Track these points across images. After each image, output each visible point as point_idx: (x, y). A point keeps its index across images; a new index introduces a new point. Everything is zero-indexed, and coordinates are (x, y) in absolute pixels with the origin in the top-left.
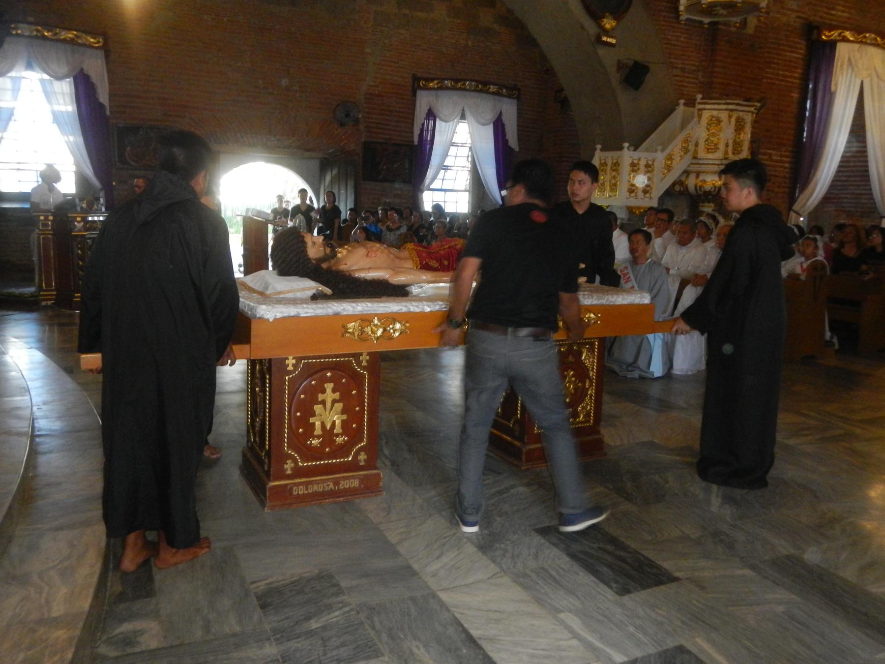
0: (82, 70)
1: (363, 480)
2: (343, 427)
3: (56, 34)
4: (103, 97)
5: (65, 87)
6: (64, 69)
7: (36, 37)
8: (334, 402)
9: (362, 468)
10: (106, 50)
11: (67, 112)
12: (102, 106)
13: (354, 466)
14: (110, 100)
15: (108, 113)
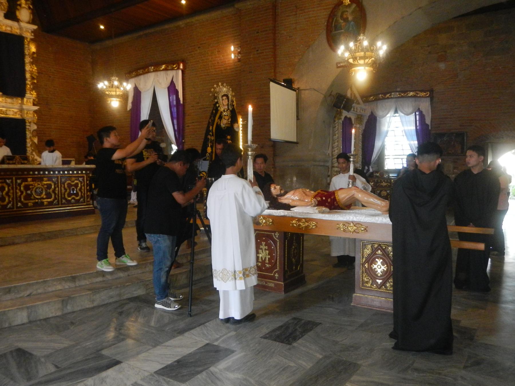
0: (419, 109)
1: (276, 285)
2: (269, 260)
3: (417, 94)
4: (428, 121)
5: (412, 117)
6: (411, 110)
7: (399, 97)
8: (265, 249)
9: (277, 280)
10: (432, 98)
11: (411, 130)
12: (428, 125)
13: (273, 278)
14: (431, 122)
15: (430, 128)
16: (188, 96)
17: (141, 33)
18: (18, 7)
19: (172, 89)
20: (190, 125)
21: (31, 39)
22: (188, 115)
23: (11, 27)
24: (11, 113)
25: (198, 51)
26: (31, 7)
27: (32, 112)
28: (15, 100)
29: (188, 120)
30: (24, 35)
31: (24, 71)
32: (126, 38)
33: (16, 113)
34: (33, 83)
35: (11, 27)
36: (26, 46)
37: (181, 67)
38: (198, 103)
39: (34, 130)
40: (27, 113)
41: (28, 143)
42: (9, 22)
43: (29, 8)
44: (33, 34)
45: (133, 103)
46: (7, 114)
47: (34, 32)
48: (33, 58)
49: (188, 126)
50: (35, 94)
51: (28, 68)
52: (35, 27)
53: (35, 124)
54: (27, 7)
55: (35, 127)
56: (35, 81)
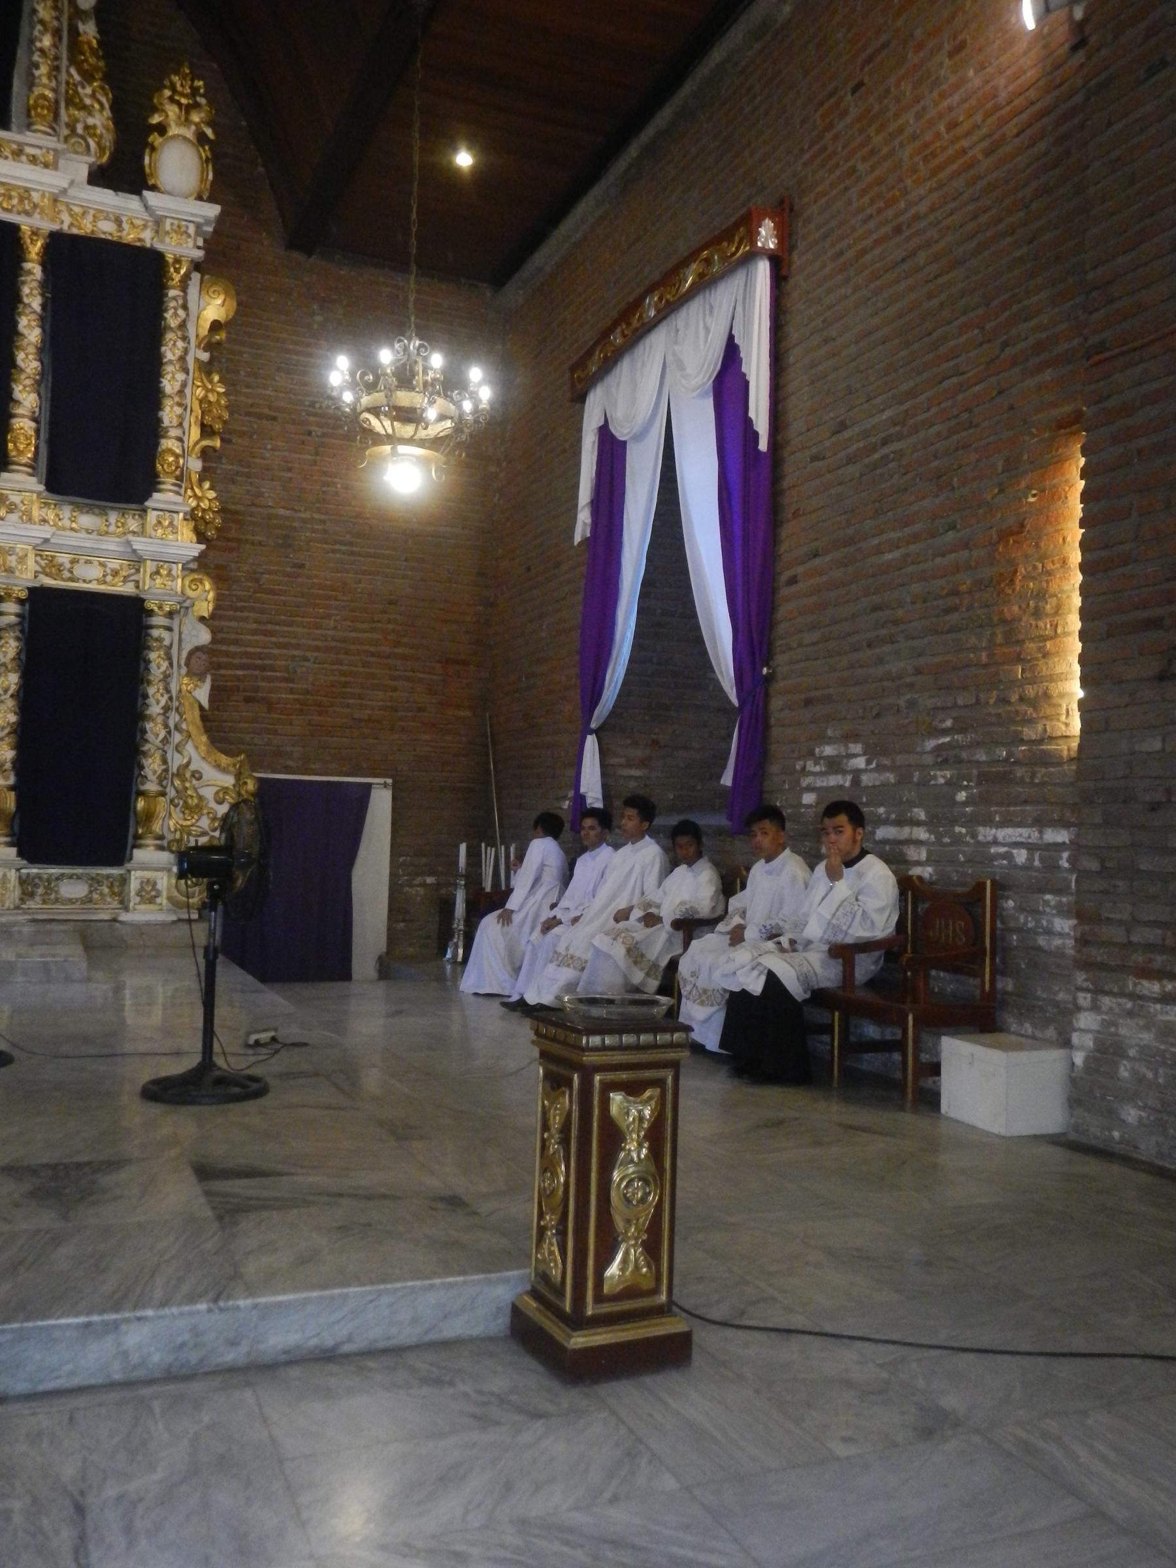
16: (798, 405)
17: (633, 150)
18: (155, 139)
19: (728, 384)
20: (800, 570)
21: (197, 266)
22: (796, 515)
23: (118, 222)
24: (95, 572)
25: (854, 112)
26: (209, 132)
27: (177, 569)
28: (113, 517)
29: (793, 540)
30: (159, 246)
31: (154, 398)
32: (585, 207)
33: (115, 573)
34: (205, 454)
35: (118, 222)
36: (172, 293)
37: (767, 236)
38: (842, 426)
39: (197, 649)
40: (157, 573)
41: (151, 701)
42: (105, 197)
43: (201, 138)
44: (200, 242)
45: (596, 505)
46: (72, 580)
48: (209, 346)
49: (793, 581)
50: (212, 494)
51: (170, 383)
54: (189, 133)
55: (204, 636)
56: (217, 443)
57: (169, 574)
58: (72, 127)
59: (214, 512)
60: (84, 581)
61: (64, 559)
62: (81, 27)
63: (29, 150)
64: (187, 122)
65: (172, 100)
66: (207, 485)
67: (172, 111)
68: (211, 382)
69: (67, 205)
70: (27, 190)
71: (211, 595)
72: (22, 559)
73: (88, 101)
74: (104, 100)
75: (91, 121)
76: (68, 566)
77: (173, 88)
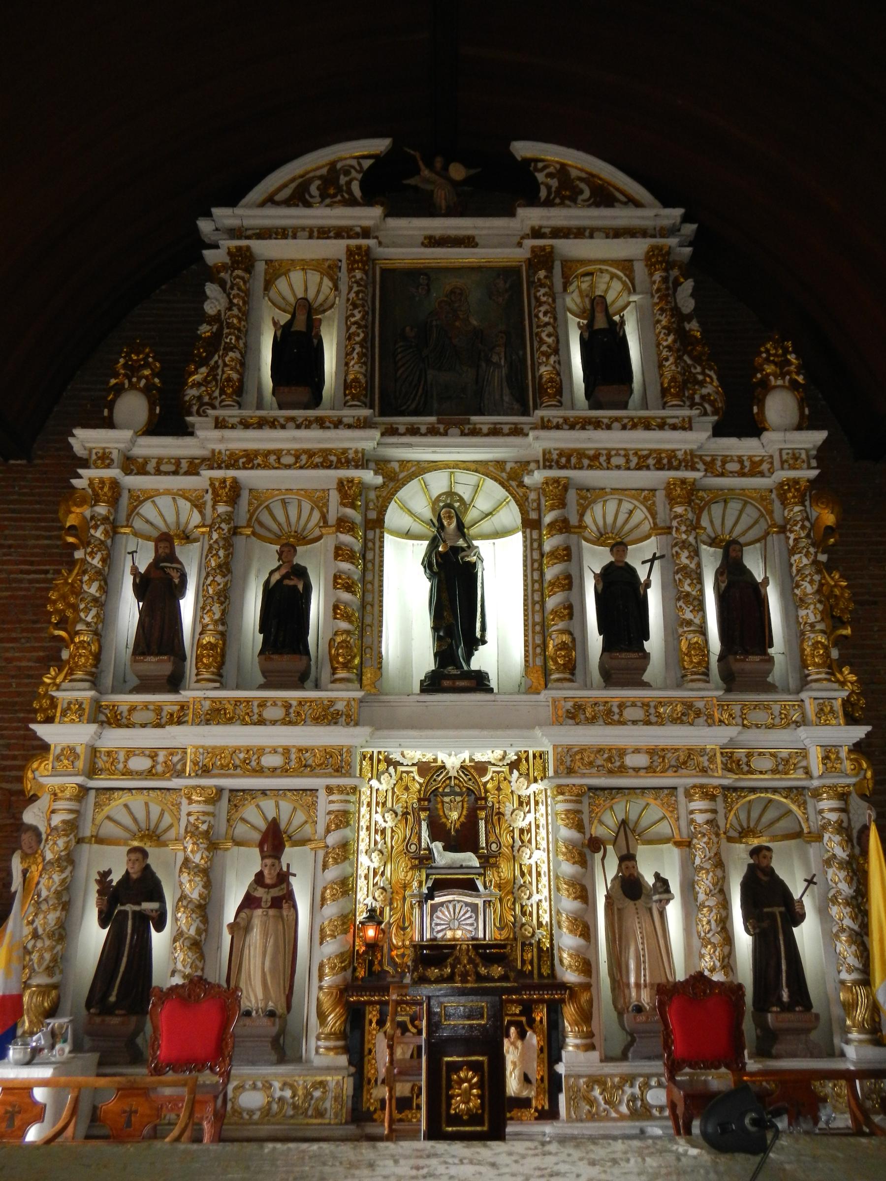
21: (812, 482)
34: (840, 642)
44: (814, 463)
47: (822, 455)
50: (853, 678)
52: (820, 436)
53: (863, 796)
56: (848, 631)
57: (838, 758)
58: (691, 398)
59: (857, 694)
60: (761, 773)
61: (741, 753)
62: (687, 326)
63: (671, 421)
64: (783, 375)
65: (767, 361)
66: (846, 670)
67: (769, 369)
68: (832, 578)
69: (700, 457)
70: (673, 451)
71: (869, 774)
72: (712, 760)
73: (700, 377)
74: (712, 373)
75: (704, 391)
76: (745, 760)
77: (767, 351)
